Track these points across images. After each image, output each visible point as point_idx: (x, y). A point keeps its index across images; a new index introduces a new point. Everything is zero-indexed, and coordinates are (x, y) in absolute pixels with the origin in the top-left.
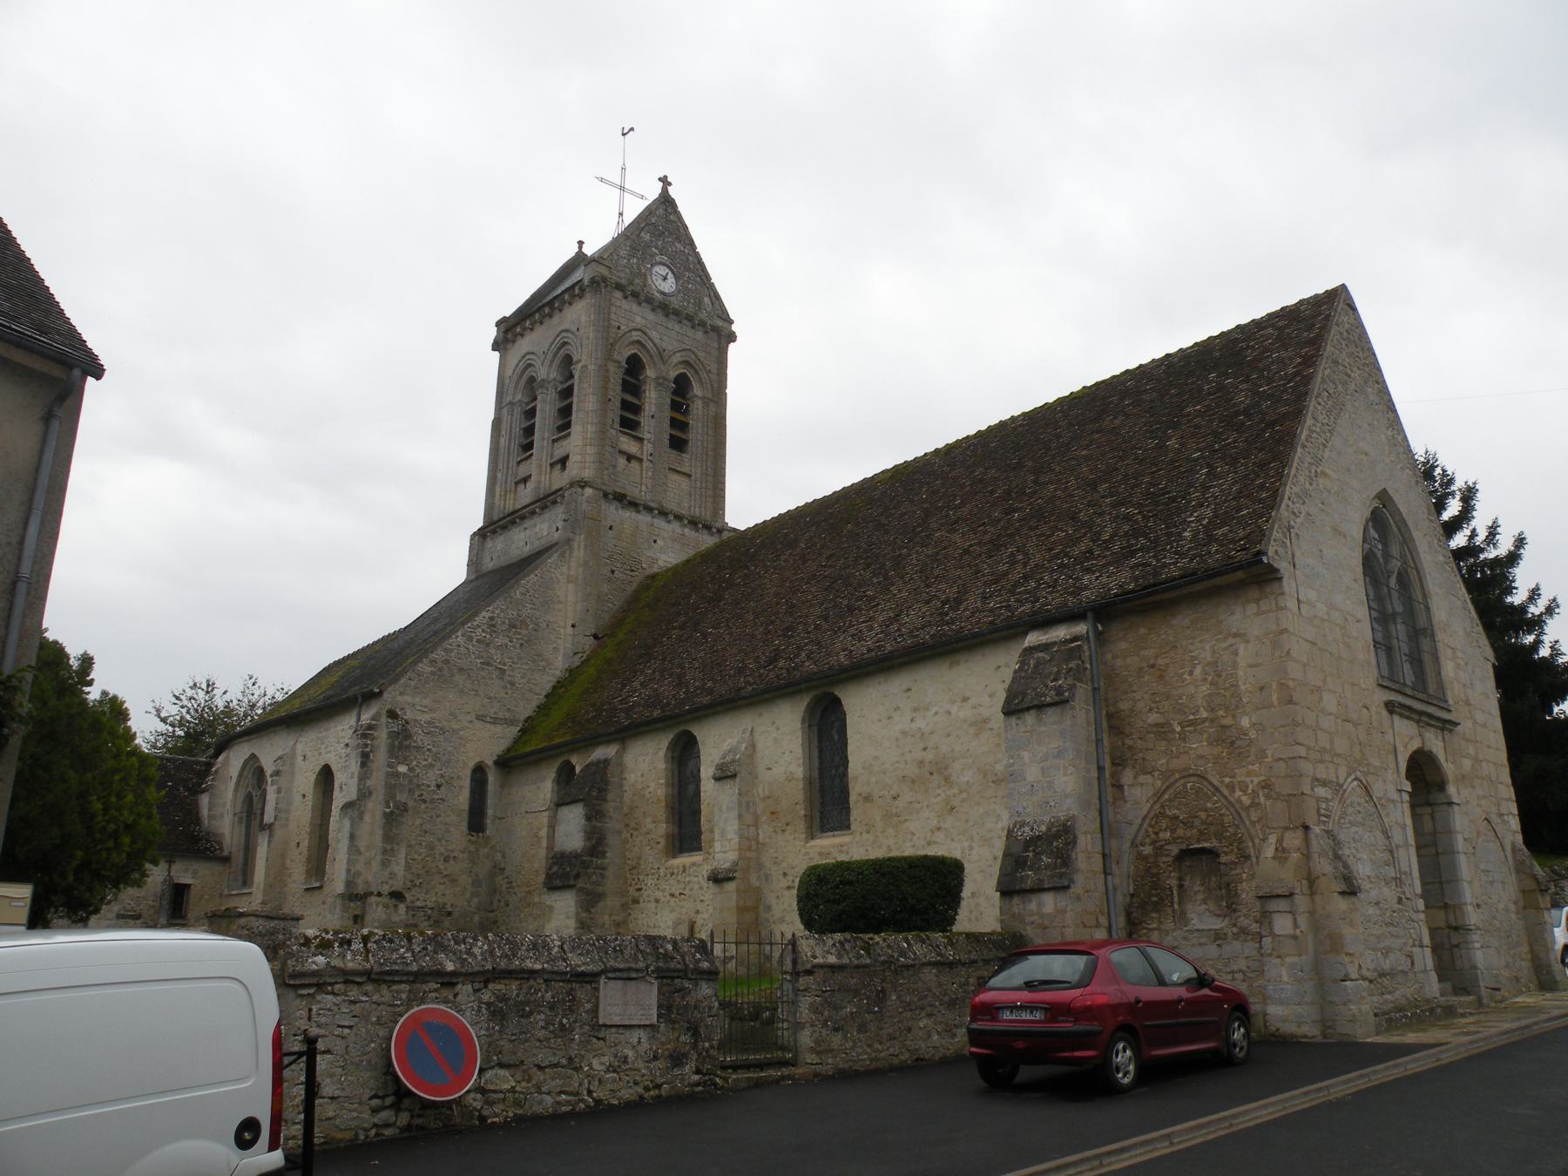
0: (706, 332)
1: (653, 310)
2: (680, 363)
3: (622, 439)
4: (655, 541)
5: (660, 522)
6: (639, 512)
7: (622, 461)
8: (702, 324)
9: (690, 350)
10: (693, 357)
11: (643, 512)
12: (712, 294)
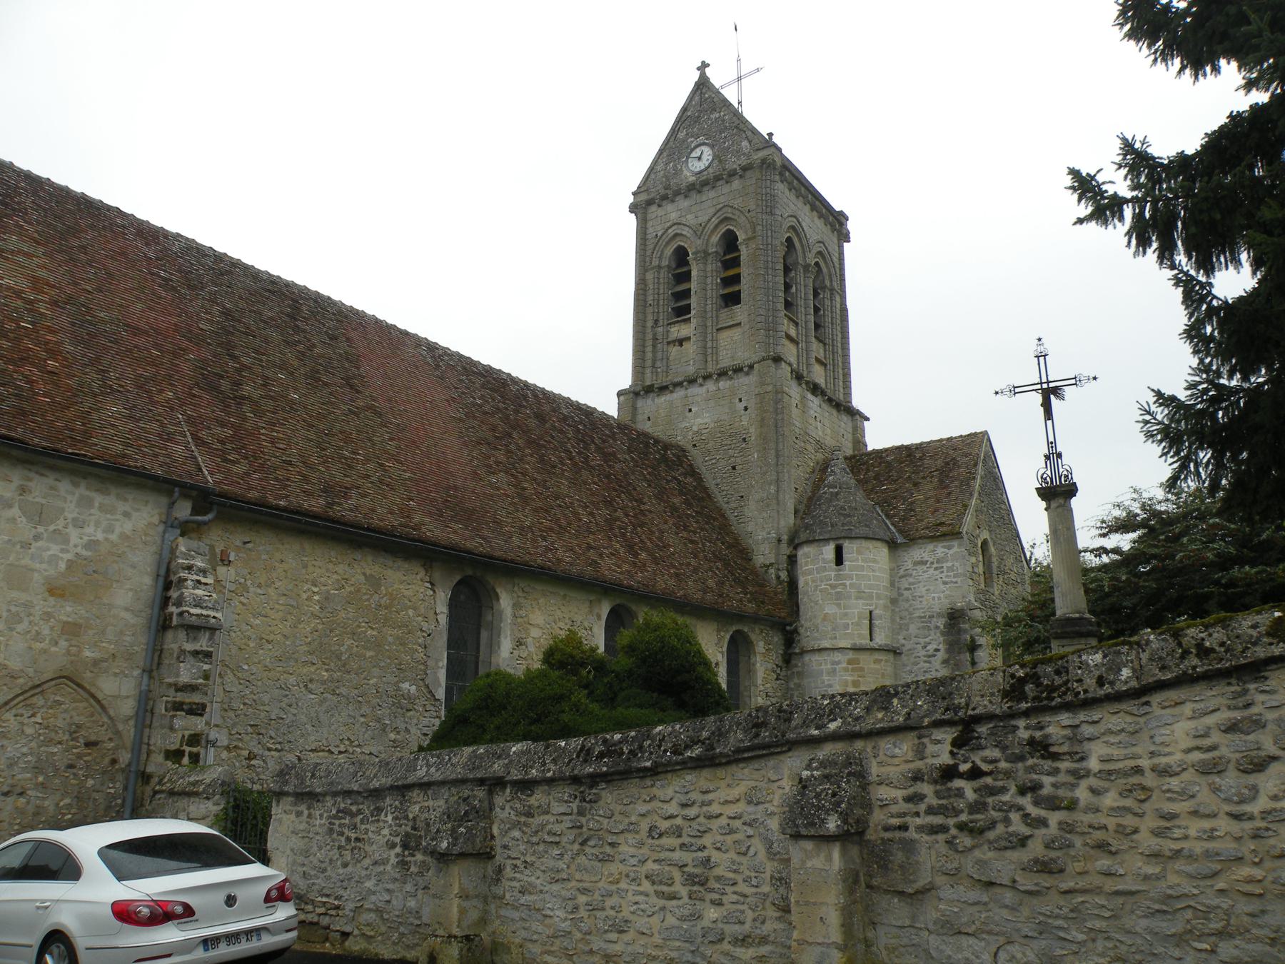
0: (741, 176)
1: (686, 197)
2: (721, 222)
3: (672, 330)
4: (690, 410)
5: (695, 390)
6: (672, 392)
7: (674, 350)
8: (732, 174)
10: (730, 210)
11: (678, 389)
12: (749, 133)
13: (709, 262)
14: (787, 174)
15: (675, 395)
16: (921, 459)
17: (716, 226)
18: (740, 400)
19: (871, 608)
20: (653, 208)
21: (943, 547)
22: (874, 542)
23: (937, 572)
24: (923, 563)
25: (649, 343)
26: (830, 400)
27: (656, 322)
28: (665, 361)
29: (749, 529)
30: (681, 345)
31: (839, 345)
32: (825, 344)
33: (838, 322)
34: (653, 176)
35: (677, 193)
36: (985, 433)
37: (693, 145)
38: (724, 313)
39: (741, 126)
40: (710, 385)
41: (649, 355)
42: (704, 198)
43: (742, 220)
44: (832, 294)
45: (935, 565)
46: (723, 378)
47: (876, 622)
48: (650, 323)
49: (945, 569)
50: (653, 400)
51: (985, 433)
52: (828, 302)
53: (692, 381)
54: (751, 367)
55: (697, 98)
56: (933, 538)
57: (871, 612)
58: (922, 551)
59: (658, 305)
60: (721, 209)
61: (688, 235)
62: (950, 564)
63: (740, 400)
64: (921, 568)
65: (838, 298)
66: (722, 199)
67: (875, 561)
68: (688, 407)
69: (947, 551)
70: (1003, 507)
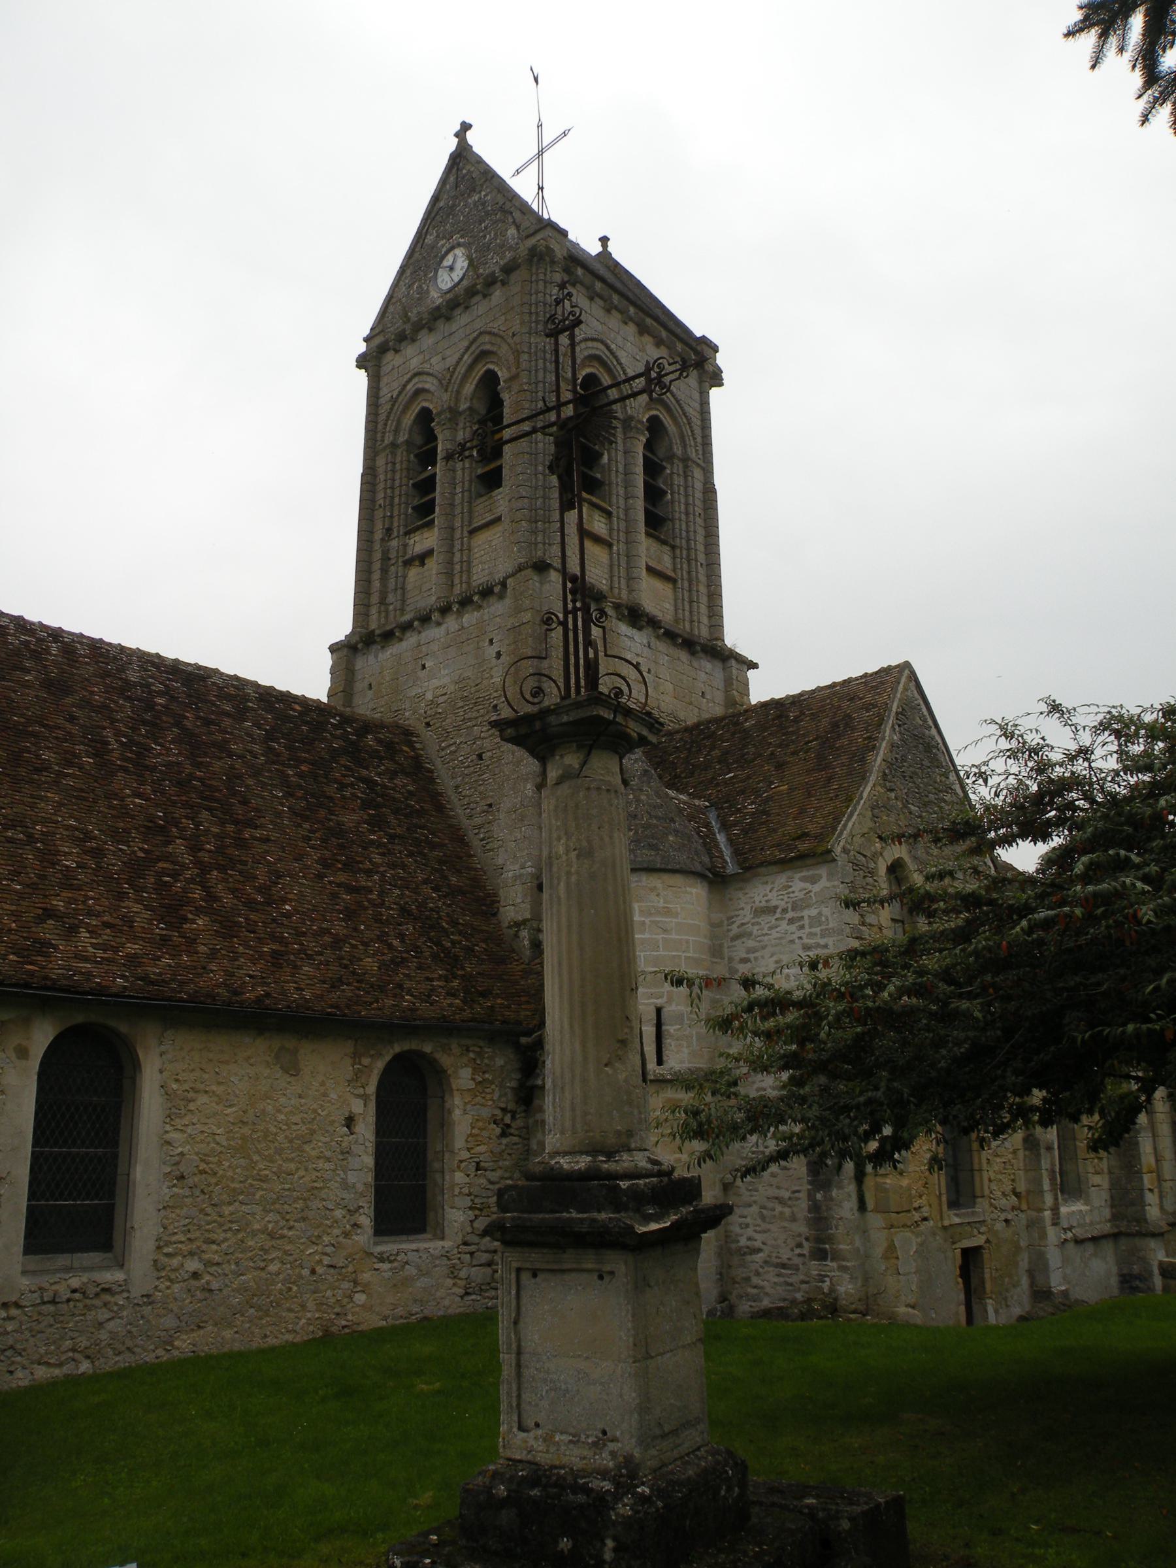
1: (431, 330)
2: (476, 361)
4: (424, 667)
5: (433, 633)
6: (401, 640)
8: (491, 282)
9: (481, 334)
10: (487, 338)
11: (408, 634)
12: (517, 215)
13: (461, 425)
14: (580, 271)
15: (404, 644)
16: (797, 720)
17: (471, 367)
18: (491, 641)
19: (659, 1002)
20: (390, 355)
21: (803, 879)
22: (666, 877)
23: (793, 928)
24: (770, 910)
25: (377, 566)
26: (670, 636)
27: (389, 531)
28: (399, 592)
29: (500, 861)
30: (423, 564)
31: (701, 548)
32: (673, 547)
33: (698, 510)
34: (391, 308)
35: (418, 327)
36: (907, 665)
37: (444, 250)
38: (480, 506)
39: (508, 205)
40: (451, 623)
41: (376, 584)
42: (454, 327)
43: (504, 350)
44: (686, 467)
45: (790, 915)
46: (469, 608)
47: (669, 1028)
48: (378, 535)
49: (806, 922)
50: (376, 657)
51: (907, 665)
52: (678, 481)
53: (425, 619)
54: (503, 584)
55: (452, 179)
56: (785, 864)
57: (659, 1011)
58: (769, 887)
59: (392, 505)
60: (475, 340)
61: (432, 389)
62: (814, 912)
63: (491, 641)
64: (766, 920)
65: (698, 474)
66: (478, 325)
67: (668, 912)
68: (420, 662)
69: (808, 886)
70: (948, 797)
